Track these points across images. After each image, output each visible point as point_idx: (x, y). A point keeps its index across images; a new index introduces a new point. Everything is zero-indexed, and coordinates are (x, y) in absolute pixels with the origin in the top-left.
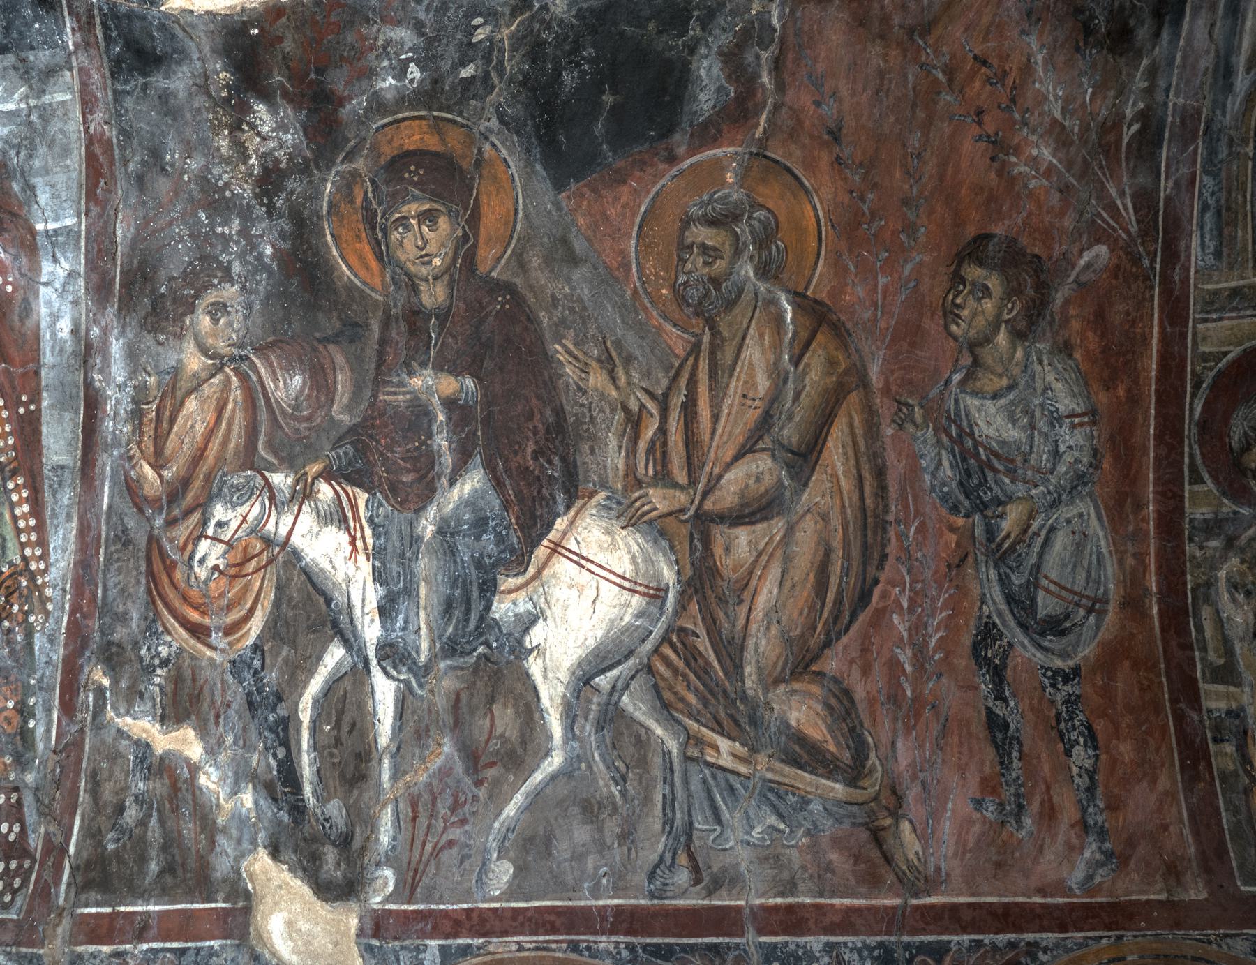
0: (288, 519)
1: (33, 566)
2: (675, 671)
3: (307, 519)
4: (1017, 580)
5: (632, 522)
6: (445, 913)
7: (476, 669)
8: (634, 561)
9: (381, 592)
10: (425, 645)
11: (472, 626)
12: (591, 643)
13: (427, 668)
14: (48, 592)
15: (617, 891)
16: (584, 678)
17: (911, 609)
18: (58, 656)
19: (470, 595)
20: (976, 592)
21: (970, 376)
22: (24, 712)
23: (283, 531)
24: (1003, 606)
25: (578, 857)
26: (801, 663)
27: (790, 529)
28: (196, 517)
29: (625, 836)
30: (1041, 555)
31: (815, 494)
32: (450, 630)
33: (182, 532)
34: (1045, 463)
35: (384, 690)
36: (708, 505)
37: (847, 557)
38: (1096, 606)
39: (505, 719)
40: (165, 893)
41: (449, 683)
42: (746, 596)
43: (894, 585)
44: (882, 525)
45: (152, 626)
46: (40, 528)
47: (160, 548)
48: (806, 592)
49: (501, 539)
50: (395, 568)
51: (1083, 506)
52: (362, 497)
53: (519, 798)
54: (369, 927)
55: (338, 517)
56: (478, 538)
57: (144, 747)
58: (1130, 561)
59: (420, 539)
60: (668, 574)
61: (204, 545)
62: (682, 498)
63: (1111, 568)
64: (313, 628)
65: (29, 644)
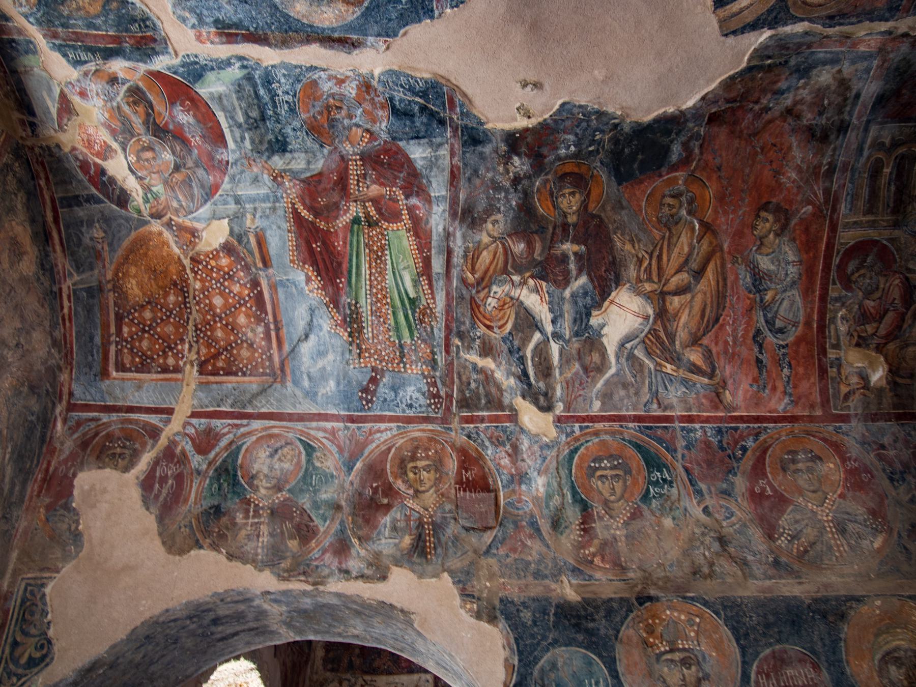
0: (518, 291)
2: (652, 342)
3: (525, 291)
4: (769, 315)
5: (639, 293)
7: (585, 341)
9: (552, 315)
10: (567, 333)
12: (624, 333)
13: (569, 341)
15: (634, 410)
16: (622, 345)
18: (443, 335)
19: (582, 317)
20: (755, 319)
21: (759, 248)
23: (517, 295)
24: (764, 324)
25: (621, 400)
26: (695, 341)
27: (693, 297)
28: (487, 290)
30: (778, 307)
31: (702, 286)
33: (482, 295)
34: (783, 277)
35: (555, 348)
36: (665, 289)
37: (712, 307)
38: (795, 324)
39: (596, 357)
40: (488, 409)
41: (576, 345)
42: (677, 319)
43: (727, 317)
44: (725, 297)
45: (473, 326)
46: (432, 293)
48: (698, 317)
49: (593, 299)
50: (556, 308)
51: (795, 292)
52: (544, 284)
55: (536, 291)
57: (475, 365)
58: (809, 310)
60: (650, 312)
61: (490, 300)
62: (656, 286)
63: (802, 312)
64: (529, 327)
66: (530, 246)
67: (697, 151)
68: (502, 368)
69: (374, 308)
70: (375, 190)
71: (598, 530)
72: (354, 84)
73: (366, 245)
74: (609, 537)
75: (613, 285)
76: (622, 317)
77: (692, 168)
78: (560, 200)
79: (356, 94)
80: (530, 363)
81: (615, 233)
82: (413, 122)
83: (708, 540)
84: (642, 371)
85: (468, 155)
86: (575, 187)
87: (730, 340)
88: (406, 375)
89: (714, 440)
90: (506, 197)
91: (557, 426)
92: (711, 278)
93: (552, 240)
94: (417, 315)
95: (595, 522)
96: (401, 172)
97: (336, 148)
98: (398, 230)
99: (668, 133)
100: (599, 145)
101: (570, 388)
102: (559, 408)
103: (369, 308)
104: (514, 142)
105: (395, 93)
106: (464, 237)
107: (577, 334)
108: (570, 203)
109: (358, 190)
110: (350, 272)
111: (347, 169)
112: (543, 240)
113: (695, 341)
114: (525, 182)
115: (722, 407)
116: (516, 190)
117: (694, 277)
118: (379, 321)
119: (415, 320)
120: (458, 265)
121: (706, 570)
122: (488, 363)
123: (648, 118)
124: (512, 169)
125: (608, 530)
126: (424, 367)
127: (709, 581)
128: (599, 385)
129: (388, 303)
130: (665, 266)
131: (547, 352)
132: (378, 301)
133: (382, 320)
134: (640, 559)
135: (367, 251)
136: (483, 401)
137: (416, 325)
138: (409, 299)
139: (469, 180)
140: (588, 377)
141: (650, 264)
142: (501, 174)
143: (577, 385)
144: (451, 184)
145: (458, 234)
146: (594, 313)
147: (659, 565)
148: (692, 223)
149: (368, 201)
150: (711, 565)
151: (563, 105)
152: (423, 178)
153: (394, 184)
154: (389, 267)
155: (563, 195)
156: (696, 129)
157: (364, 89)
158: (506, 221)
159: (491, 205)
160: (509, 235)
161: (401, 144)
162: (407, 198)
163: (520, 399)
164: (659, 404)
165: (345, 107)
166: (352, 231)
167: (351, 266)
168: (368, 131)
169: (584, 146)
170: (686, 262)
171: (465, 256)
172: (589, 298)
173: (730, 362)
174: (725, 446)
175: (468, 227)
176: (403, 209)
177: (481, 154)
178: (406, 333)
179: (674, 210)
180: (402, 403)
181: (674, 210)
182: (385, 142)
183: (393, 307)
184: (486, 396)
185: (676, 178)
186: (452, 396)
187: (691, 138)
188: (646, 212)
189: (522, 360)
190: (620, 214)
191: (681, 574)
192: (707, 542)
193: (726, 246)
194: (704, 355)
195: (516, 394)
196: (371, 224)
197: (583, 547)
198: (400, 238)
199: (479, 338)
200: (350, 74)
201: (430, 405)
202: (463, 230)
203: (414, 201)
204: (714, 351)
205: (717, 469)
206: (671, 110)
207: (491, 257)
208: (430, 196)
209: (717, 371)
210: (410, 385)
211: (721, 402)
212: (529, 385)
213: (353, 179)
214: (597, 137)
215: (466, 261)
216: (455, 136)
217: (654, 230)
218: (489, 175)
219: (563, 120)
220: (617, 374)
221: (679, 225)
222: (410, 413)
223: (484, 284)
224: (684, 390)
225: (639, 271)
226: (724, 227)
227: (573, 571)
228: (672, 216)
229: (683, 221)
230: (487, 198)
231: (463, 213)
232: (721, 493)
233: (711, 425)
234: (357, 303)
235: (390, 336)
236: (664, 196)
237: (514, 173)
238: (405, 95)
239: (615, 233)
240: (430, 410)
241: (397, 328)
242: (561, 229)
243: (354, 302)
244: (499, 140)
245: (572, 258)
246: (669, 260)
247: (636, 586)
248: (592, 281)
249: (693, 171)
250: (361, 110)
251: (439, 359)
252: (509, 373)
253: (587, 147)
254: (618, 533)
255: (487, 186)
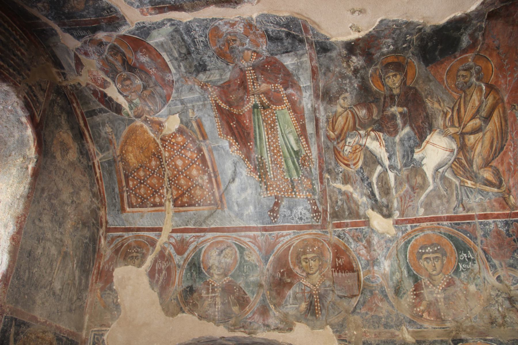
0: (365, 140)
1: (308, 155)
3: (369, 140)
5: (446, 135)
6: (410, 219)
7: (411, 169)
8: (446, 144)
9: (388, 154)
10: (399, 165)
11: (409, 160)
12: (437, 162)
13: (400, 170)
14: (313, 160)
15: (447, 213)
16: (436, 170)
17: (513, 151)
18: (318, 172)
19: (409, 153)
22: (313, 184)
23: (364, 143)
25: (438, 207)
26: (487, 164)
27: (484, 135)
28: (344, 141)
29: (448, 202)
31: (490, 126)
32: (405, 161)
33: (341, 145)
35: (391, 175)
36: (464, 131)
37: (498, 140)
39: (419, 180)
40: (350, 218)
41: (406, 173)
42: (473, 150)
44: (507, 133)
45: (337, 165)
46: (308, 146)
47: (337, 149)
49: (414, 141)
50: (390, 149)
52: (381, 134)
53: (424, 196)
54: (395, 223)
55: (377, 139)
56: (409, 141)
57: (340, 190)
59: (395, 142)
60: (454, 146)
61: (346, 147)
62: (457, 130)
65: (311, 171)
66: (370, 111)
67: (480, 38)
68: (357, 191)
69: (273, 159)
70: (264, 87)
71: (425, 295)
72: (241, 25)
73: (264, 121)
74: (432, 299)
75: (428, 131)
76: (436, 151)
77: (478, 50)
78: (387, 80)
79: (244, 30)
80: (375, 186)
81: (427, 98)
82: (283, 43)
83: (500, 299)
84: (451, 186)
85: (321, 59)
86: (396, 71)
87: (512, 161)
88: (296, 199)
89: (503, 230)
90: (350, 82)
91: (396, 227)
92: (496, 121)
93: (384, 106)
94: (300, 161)
95: (423, 290)
96: (280, 74)
97: (236, 64)
98: (282, 109)
99: (458, 29)
100: (410, 42)
101: (403, 201)
102: (397, 215)
103: (270, 159)
104: (351, 47)
105: (268, 27)
106: (325, 109)
107: (405, 165)
108: (394, 81)
109: (254, 88)
110: (255, 138)
111: (245, 76)
112: (378, 106)
113: (487, 164)
114: (362, 71)
115: (508, 207)
116: (356, 77)
117: (484, 121)
118: (277, 167)
119: (299, 164)
120: (323, 128)
121: (500, 321)
122: (349, 188)
123: (442, 21)
124: (352, 64)
125: (432, 294)
126: (308, 193)
127: (502, 328)
128: (422, 198)
129: (281, 155)
130: (463, 116)
131: (386, 179)
132: (275, 154)
133: (278, 166)
134: (454, 314)
135: (265, 124)
136: (347, 213)
137: (300, 167)
138: (294, 151)
139: (325, 74)
140: (415, 193)
141: (452, 115)
142: (346, 68)
143: (407, 199)
144: (313, 78)
145: (321, 108)
146: (416, 150)
147: (467, 318)
148: (480, 86)
149: (261, 94)
150: (504, 317)
151: (381, 21)
152: (294, 76)
153: (276, 82)
154: (279, 132)
155: (389, 77)
156: (479, 24)
157: (248, 27)
158: (352, 97)
159: (341, 88)
160: (354, 106)
161: (277, 57)
162: (285, 89)
163: (370, 211)
164: (464, 207)
165: (238, 39)
166: (254, 113)
167: (256, 134)
168: (255, 52)
169: (400, 45)
170: (478, 112)
171: (327, 121)
172: (412, 141)
173: (512, 177)
174: (511, 233)
175: (327, 103)
176: (284, 97)
177: (330, 57)
178: (294, 173)
179: (467, 79)
180: (295, 217)
181: (467, 79)
182: (267, 57)
183: (285, 157)
184: (349, 209)
185: (466, 58)
186: (327, 211)
187: (475, 31)
188: (447, 82)
189: (370, 185)
190: (429, 85)
191: (482, 324)
192: (500, 301)
193: (506, 99)
194: (494, 173)
195: (368, 207)
196: (265, 107)
197: (416, 306)
198: (284, 115)
199: (341, 172)
200: (238, 19)
201: (313, 217)
202: (324, 105)
203: (290, 91)
204: (501, 170)
205: (506, 250)
206: (459, 14)
207: (345, 120)
208: (300, 87)
209: (504, 183)
210: (300, 205)
211: (507, 204)
212: (376, 201)
213: (250, 82)
214: (408, 38)
215: (328, 124)
216: (311, 48)
217: (454, 93)
218: (337, 69)
219: (383, 31)
220: (434, 190)
221: (471, 88)
222: (301, 223)
223: (342, 137)
224: (481, 197)
225: (445, 120)
226: (504, 87)
227: (409, 322)
228: (466, 83)
229: (473, 85)
230: (338, 84)
231: (323, 96)
232: (510, 266)
233: (500, 220)
234: (262, 157)
235: (285, 176)
236: (458, 71)
237: (354, 67)
238: (275, 27)
239: (427, 98)
240: (313, 220)
241: (289, 171)
242: (389, 98)
243: (260, 156)
244: (341, 48)
245: (399, 116)
246: (465, 112)
247: (452, 332)
248: (413, 130)
249: (479, 52)
250: (248, 40)
251: (317, 188)
252: (363, 194)
253: (402, 45)
254: (439, 296)
255: (337, 76)
